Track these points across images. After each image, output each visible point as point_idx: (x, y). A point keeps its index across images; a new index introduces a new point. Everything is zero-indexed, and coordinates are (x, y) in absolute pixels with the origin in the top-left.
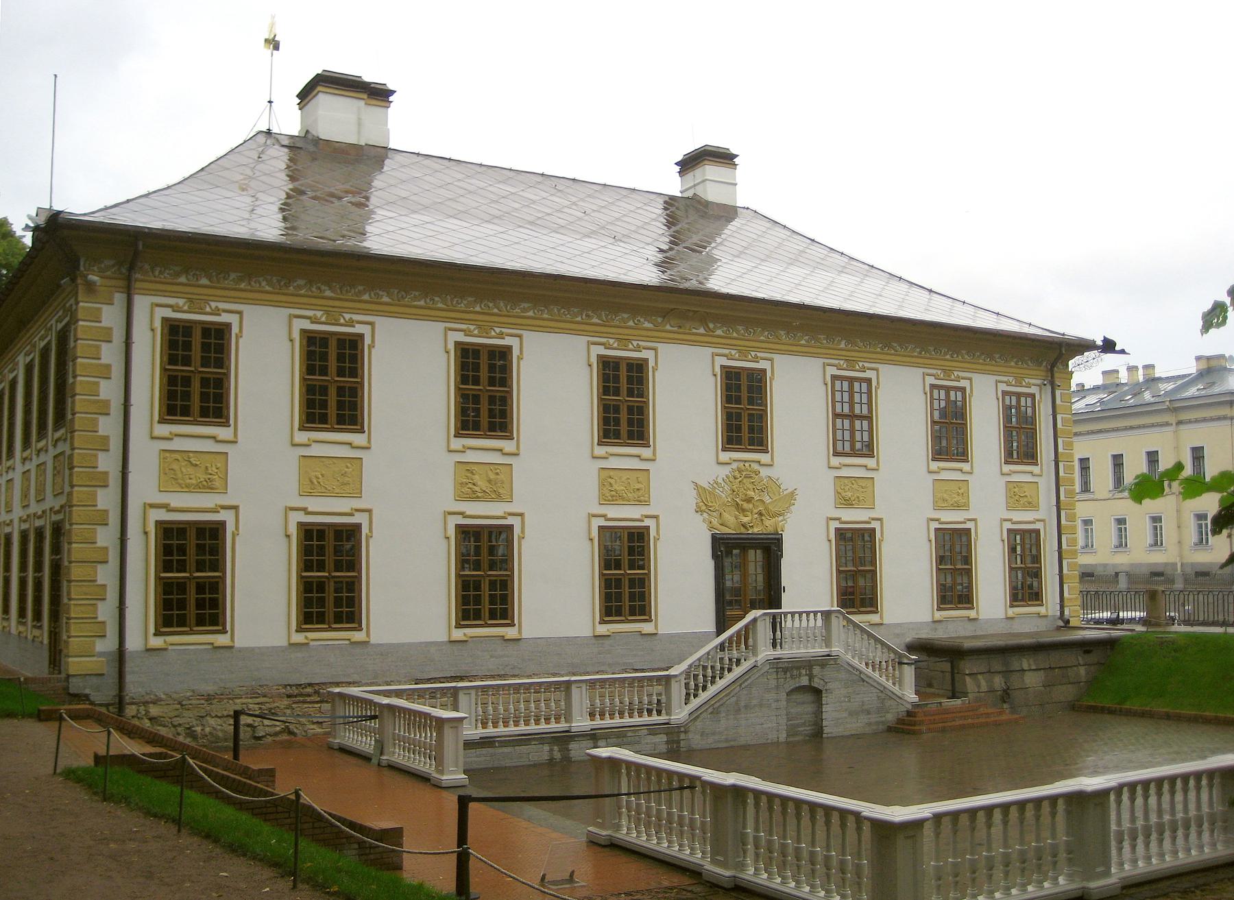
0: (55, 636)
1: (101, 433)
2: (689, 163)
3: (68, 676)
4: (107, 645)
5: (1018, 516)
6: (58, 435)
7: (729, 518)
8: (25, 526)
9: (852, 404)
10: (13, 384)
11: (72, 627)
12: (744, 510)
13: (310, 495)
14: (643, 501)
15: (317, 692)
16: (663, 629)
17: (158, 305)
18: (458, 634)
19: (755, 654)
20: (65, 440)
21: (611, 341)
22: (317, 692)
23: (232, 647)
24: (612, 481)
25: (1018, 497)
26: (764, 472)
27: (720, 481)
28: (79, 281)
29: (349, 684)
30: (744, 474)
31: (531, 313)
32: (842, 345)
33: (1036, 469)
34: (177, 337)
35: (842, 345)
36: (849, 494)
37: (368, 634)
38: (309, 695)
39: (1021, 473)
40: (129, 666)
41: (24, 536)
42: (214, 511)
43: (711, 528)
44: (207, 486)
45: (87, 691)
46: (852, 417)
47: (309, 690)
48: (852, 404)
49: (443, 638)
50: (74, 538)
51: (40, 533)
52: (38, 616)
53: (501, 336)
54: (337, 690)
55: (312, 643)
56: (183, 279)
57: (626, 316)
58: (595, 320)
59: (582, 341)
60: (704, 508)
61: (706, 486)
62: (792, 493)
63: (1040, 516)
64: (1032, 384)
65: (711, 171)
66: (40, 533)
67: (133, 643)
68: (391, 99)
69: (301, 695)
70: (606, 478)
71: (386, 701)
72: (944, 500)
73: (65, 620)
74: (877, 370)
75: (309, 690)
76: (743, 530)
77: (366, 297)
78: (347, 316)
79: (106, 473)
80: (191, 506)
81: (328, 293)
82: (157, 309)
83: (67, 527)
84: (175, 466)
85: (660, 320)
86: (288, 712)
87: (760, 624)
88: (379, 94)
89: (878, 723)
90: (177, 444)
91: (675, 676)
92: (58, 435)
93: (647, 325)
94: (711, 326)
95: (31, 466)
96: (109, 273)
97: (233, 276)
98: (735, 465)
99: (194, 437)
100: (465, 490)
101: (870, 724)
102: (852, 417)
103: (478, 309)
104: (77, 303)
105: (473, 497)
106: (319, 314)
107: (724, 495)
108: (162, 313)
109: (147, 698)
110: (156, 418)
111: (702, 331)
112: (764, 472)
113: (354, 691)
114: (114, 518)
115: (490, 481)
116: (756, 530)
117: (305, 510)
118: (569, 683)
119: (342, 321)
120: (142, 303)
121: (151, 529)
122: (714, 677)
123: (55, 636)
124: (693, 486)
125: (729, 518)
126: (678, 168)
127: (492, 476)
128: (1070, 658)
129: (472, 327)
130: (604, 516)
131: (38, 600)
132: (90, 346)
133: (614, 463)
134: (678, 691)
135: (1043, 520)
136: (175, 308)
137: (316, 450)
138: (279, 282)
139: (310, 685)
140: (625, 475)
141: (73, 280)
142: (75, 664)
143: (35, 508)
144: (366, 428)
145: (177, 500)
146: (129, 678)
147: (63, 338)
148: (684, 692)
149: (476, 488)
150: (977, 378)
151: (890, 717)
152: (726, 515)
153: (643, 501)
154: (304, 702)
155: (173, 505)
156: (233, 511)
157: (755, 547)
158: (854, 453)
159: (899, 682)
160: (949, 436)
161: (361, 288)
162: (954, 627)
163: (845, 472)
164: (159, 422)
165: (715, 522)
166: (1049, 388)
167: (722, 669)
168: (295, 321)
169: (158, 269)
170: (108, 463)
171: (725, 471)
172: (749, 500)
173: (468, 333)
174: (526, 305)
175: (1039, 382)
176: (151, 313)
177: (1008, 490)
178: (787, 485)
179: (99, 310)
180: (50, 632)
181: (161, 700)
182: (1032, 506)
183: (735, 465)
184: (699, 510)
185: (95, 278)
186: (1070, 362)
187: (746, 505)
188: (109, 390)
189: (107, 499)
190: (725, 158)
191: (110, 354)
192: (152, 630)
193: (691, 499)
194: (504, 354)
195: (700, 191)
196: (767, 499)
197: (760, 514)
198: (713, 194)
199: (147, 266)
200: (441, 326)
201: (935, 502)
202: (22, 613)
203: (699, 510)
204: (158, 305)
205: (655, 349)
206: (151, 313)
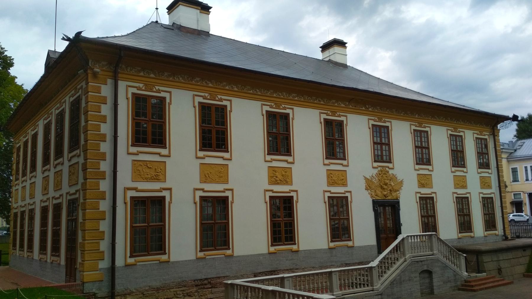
0: (71, 261)
1: (101, 151)
2: (325, 47)
3: (83, 283)
4: (104, 264)
6: (56, 162)
8: (43, 204)
10: (35, 137)
11: (86, 255)
12: (384, 189)
13: (205, 182)
14: (345, 185)
15: (210, 283)
16: (356, 244)
17: (130, 86)
18: (272, 249)
19: (404, 254)
20: (79, 156)
21: (329, 112)
22: (210, 283)
23: (169, 262)
24: (332, 176)
25: (485, 183)
26: (391, 172)
27: (374, 176)
28: (89, 71)
30: (383, 173)
31: (296, 99)
32: (417, 116)
33: (490, 171)
34: (139, 103)
35: (417, 116)
36: (423, 182)
38: (206, 285)
39: (485, 173)
40: (117, 274)
41: (44, 210)
42: (160, 191)
43: (372, 197)
44: (156, 178)
45: (94, 290)
47: (206, 282)
49: (266, 251)
50: (87, 207)
51: (58, 208)
52: (56, 249)
53: (285, 108)
54: (229, 282)
55: (207, 257)
56: (142, 74)
57: (334, 101)
58: (322, 103)
59: (317, 112)
61: (369, 178)
62: (402, 181)
63: (493, 191)
64: (486, 136)
65: (336, 49)
67: (119, 262)
69: (202, 285)
70: (330, 174)
71: (271, 288)
72: (458, 184)
73: (79, 252)
75: (206, 282)
77: (227, 88)
78: (219, 97)
79: (105, 172)
80: (148, 188)
81: (210, 85)
82: (129, 88)
83: (82, 201)
84: (140, 168)
85: (347, 103)
86: (196, 294)
87: (405, 241)
89: (454, 287)
90: (141, 157)
91: (374, 267)
92: (56, 162)
93: (342, 105)
94: (367, 106)
95: (51, 174)
96: (104, 68)
97: (166, 74)
98: (379, 169)
99: (149, 154)
100: (273, 179)
101: (451, 287)
103: (275, 95)
104: (87, 83)
105: (276, 183)
106: (207, 95)
107: (375, 181)
108: (131, 90)
109: (126, 292)
110: (130, 144)
111: (364, 108)
112: (391, 172)
113: (238, 281)
114: (109, 196)
115: (283, 175)
116: (389, 198)
117: (203, 190)
118: (331, 273)
119: (217, 99)
120: (122, 85)
121: (128, 200)
122: (388, 267)
123: (71, 261)
124: (363, 178)
125: (379, 193)
126: (321, 49)
127: (284, 173)
128: (520, 253)
129: (273, 104)
132: (95, 105)
133: (332, 167)
134: (375, 273)
135: (494, 193)
137: (208, 161)
138: (188, 78)
139: (206, 279)
140: (337, 173)
141: (86, 71)
142: (88, 275)
143: (52, 193)
144: (229, 150)
145: (141, 186)
146: (117, 281)
147: (76, 106)
148: (378, 274)
149: (278, 179)
150: (467, 131)
151: (459, 283)
153: (345, 185)
154: (204, 288)
155: (139, 188)
156: (169, 191)
157: (388, 206)
159: (460, 267)
160: (458, 158)
161: (225, 83)
163: (421, 172)
164: (132, 146)
166: (492, 136)
167: (391, 263)
168: (196, 97)
169: (129, 68)
170: (105, 166)
171: (375, 171)
172: (386, 184)
173: (271, 107)
174: (295, 95)
175: (488, 134)
176: (127, 90)
177: (481, 180)
178: (400, 177)
179: (100, 87)
180: (67, 259)
181: (133, 292)
182: (489, 187)
183: (379, 169)
185: (98, 70)
186: (499, 126)
187: (385, 187)
188: (106, 129)
189: (105, 186)
190: (342, 44)
191: (106, 110)
192: (128, 255)
194: (286, 117)
195: (333, 58)
196: (392, 184)
197: (391, 191)
198: (338, 59)
199: (123, 66)
200: (259, 103)
201: (455, 185)
202: (43, 248)
204: (130, 86)
205: (346, 116)
206: (127, 90)
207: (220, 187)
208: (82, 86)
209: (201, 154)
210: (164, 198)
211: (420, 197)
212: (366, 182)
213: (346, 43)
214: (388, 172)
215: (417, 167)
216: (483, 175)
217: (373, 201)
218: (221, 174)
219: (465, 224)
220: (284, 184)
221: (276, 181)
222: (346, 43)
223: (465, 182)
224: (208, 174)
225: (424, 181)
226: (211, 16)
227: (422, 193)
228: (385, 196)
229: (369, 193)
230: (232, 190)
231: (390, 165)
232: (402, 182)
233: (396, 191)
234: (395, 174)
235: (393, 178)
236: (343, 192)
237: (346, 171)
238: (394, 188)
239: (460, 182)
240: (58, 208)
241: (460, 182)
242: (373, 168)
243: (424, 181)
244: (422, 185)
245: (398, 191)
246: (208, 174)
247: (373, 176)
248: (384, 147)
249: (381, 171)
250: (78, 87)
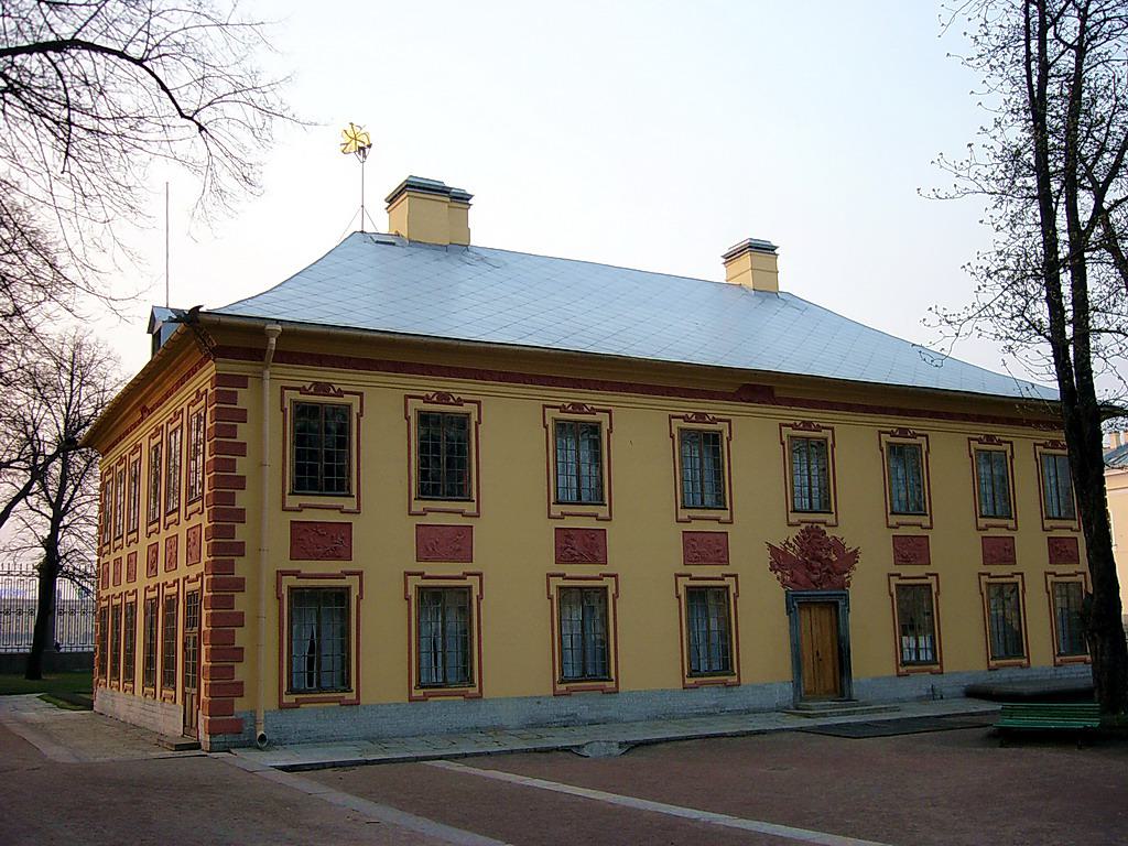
5: (1061, 569)
8: (151, 595)
12: (813, 568)
17: (287, 388)
27: (791, 541)
29: (800, 730)
37: (481, 690)
41: (151, 608)
60: (777, 567)
62: (856, 551)
66: (171, 604)
68: (470, 202)
74: (927, 436)
88: (462, 199)
90: (306, 516)
95: (161, 539)
98: (803, 527)
119: (451, 400)
121: (285, 592)
125: (801, 578)
130: (689, 576)
131: (169, 664)
136: (303, 391)
137: (431, 519)
153: (723, 559)
162: (1008, 675)
171: (796, 532)
178: (850, 546)
193: (766, 558)
207: (456, 569)
208: (206, 390)
209: (418, 506)
210: (348, 589)
213: (776, 248)
216: (1056, 534)
218: (457, 544)
219: (1009, 640)
220: (589, 562)
221: (573, 555)
222: (776, 248)
223: (1012, 551)
224: (432, 544)
225: (911, 550)
226: (471, 212)
230: (480, 575)
231: (830, 519)
235: (837, 546)
237: (726, 533)
239: (998, 551)
240: (171, 604)
241: (998, 551)
243: (911, 550)
246: (433, 544)
247: (787, 543)
250: (202, 390)
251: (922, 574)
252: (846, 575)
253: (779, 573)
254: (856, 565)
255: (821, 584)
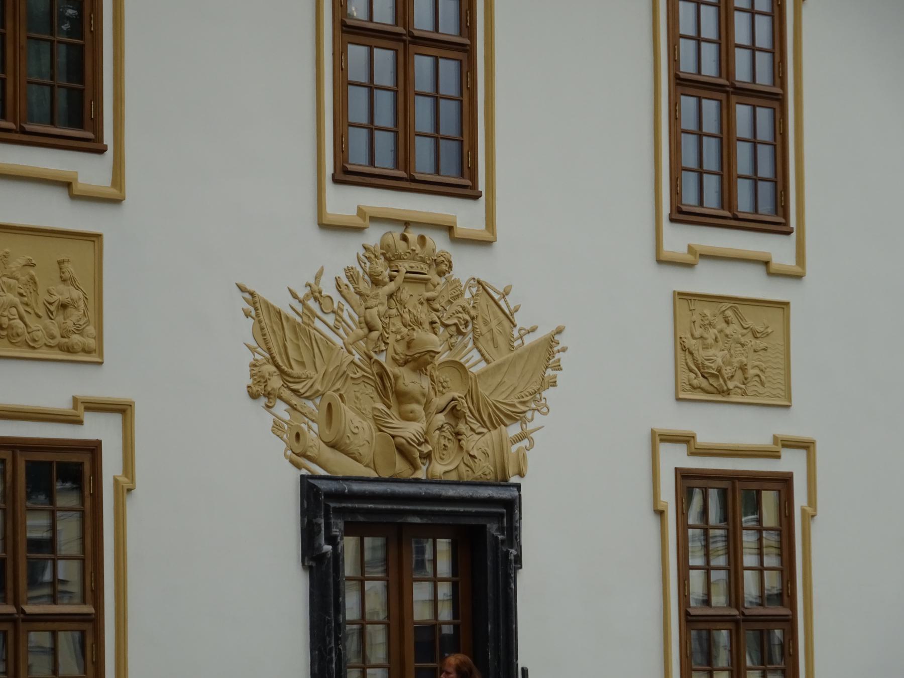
7: (358, 420)
9: (725, 44)
12: (402, 397)
26: (466, 266)
27: (328, 288)
30: (401, 268)
36: (717, 356)
43: (299, 455)
46: (727, 91)
48: (725, 44)
60: (276, 383)
61: (284, 303)
62: (550, 344)
76: (401, 467)
98: (374, 236)
102: (727, 91)
107: (338, 333)
112: (466, 266)
116: (439, 468)
124: (241, 302)
125: (357, 423)
152: (348, 415)
153: (79, 346)
158: (728, 218)
165: (312, 433)
171: (343, 255)
172: (419, 361)
178: (535, 316)
183: (374, 236)
184: (259, 391)
187: (409, 380)
193: (234, 350)
196: (473, 361)
197: (454, 412)
203: (259, 391)
211: (684, 477)
212: (261, 332)
214: (443, 266)
215: (680, 239)
217: (310, 491)
225: (725, 353)
227: (704, 439)
228: (403, 452)
229: (277, 428)
232: (550, 344)
233: (498, 418)
234: (496, 283)
236: (61, 403)
238: (483, 390)
242: (326, 226)
244: (706, 382)
245: (513, 418)
247: (316, 295)
248: (422, 65)
249: (390, 257)
251: (763, 440)
252: (514, 430)
253: (281, 409)
254: (548, 393)
255: (427, 456)
